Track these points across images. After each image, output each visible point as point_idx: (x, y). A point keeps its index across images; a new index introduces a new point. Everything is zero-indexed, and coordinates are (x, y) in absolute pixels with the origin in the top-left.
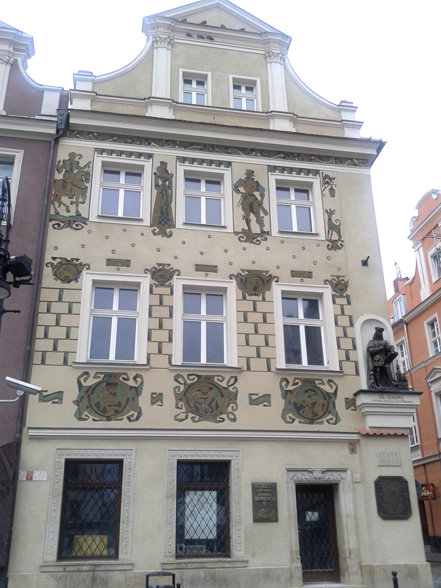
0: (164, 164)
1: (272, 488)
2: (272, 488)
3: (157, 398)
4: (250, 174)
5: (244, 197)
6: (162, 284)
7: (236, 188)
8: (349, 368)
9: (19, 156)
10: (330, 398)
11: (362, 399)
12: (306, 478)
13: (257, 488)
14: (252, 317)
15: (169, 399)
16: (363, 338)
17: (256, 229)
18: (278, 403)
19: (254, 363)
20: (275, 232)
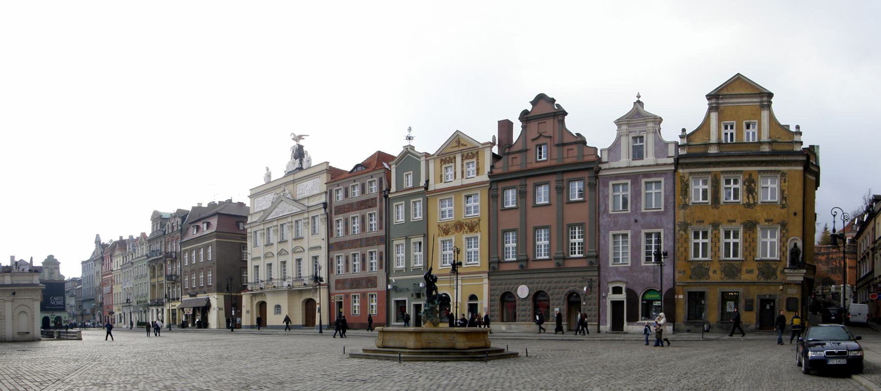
0: (715, 176)
1: (752, 301)
2: (752, 301)
3: (715, 272)
4: (750, 175)
5: (748, 187)
6: (716, 229)
7: (744, 183)
8: (783, 259)
9: (662, 180)
10: (775, 271)
11: (786, 271)
12: (764, 298)
13: (746, 301)
14: (749, 240)
15: (718, 272)
16: (790, 245)
17: (751, 201)
18: (756, 272)
19: (748, 258)
20: (759, 203)
